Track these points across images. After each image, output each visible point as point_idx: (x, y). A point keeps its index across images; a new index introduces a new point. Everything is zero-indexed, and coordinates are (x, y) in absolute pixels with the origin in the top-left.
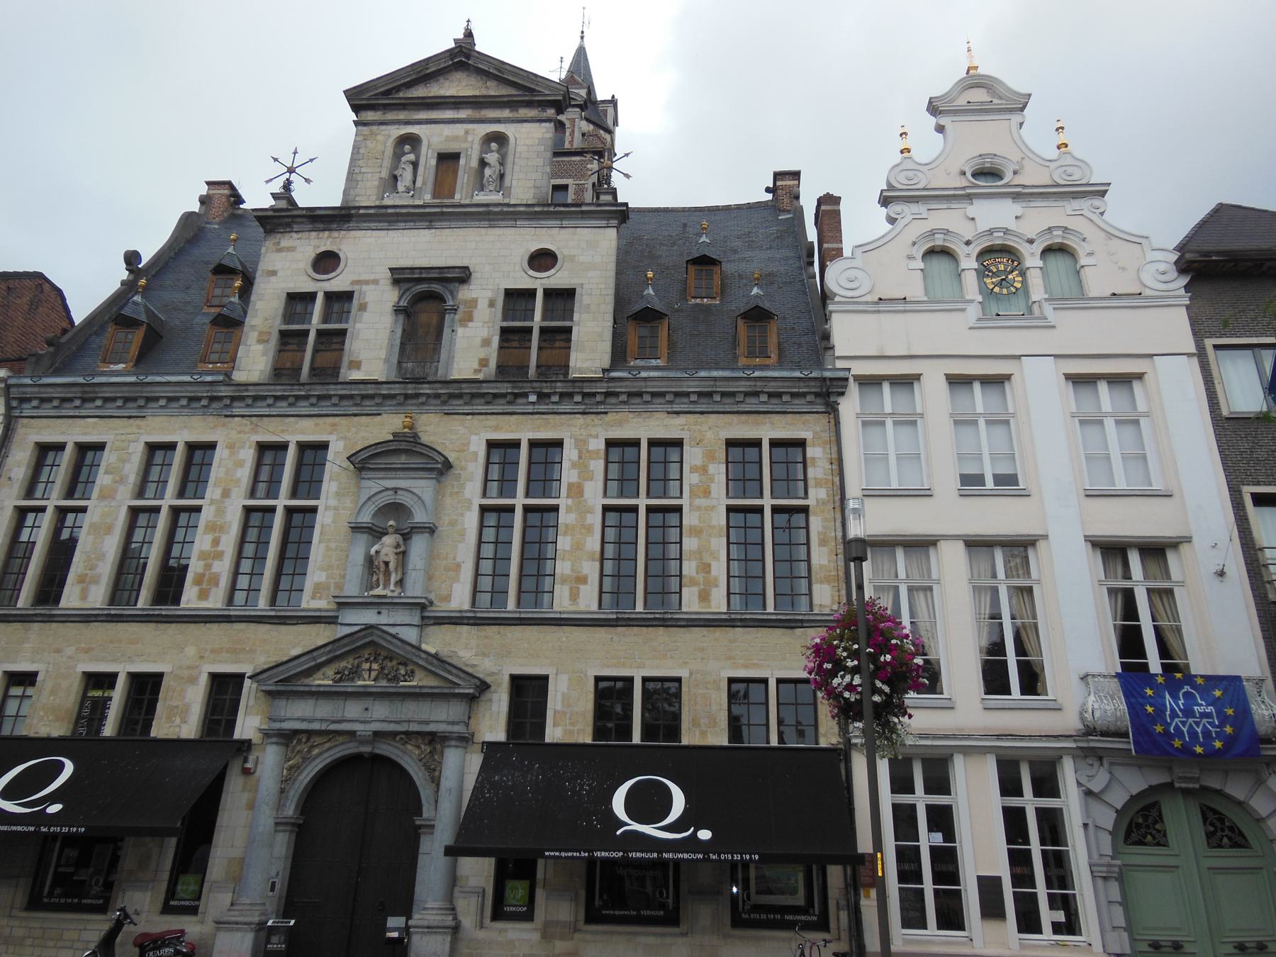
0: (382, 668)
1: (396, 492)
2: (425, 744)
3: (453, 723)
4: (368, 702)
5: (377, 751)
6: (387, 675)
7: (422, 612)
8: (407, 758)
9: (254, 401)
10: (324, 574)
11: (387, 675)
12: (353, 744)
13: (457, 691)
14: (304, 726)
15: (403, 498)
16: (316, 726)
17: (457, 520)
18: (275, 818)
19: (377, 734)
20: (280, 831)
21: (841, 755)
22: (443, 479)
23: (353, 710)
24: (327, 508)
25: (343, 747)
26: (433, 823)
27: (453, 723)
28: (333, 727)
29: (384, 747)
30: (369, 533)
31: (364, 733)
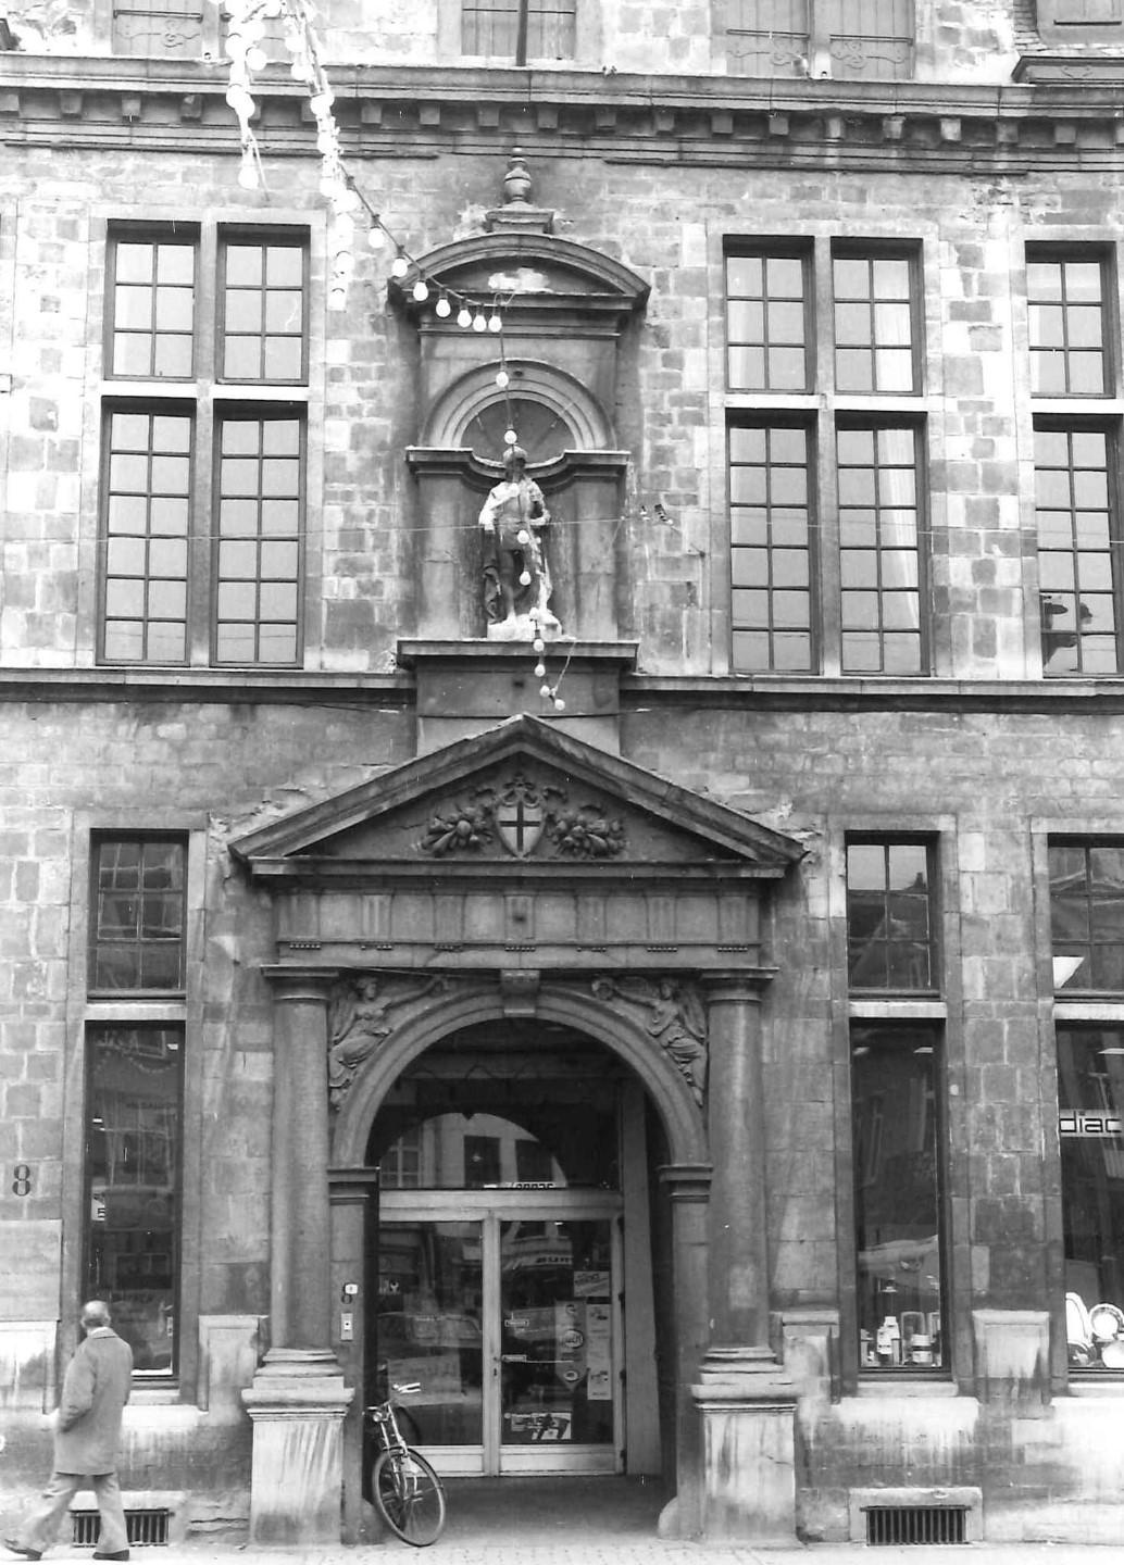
0: (550, 820)
1: (519, 374)
2: (663, 998)
3: (736, 948)
4: (521, 901)
5: (546, 1016)
6: (562, 835)
7: (621, 680)
8: (621, 1030)
9: (85, 105)
10: (350, 582)
11: (562, 835)
12: (487, 1001)
13: (744, 874)
14: (371, 958)
15: (541, 388)
16: (400, 958)
17: (672, 450)
18: (330, 1172)
19: (550, 975)
20: (344, 1202)
21: (1013, 1071)
22: (629, 337)
23: (484, 917)
24: (331, 411)
25: (454, 1011)
26: (707, 1177)
27: (736, 948)
28: (444, 960)
29: (556, 1003)
30: (464, 482)
31: (521, 974)
